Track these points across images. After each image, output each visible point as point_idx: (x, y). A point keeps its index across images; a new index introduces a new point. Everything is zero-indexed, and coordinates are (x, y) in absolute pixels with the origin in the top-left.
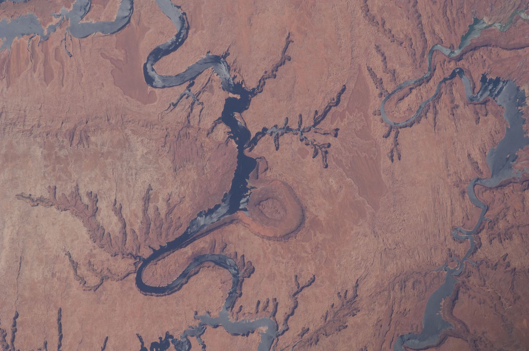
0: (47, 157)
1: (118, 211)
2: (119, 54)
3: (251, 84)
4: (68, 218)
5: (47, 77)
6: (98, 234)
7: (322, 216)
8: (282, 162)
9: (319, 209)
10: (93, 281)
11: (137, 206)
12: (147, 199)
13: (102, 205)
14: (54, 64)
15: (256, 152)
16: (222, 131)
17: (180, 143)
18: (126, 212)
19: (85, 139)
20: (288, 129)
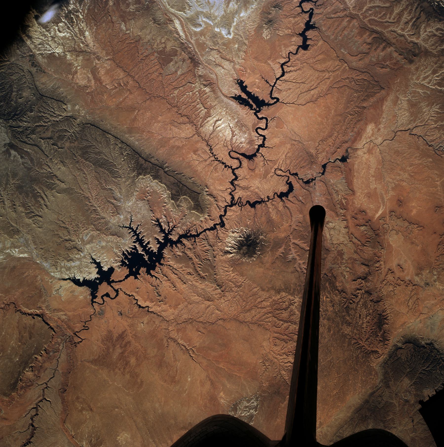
0: (236, 122)
1: (236, 140)
2: (256, 122)
3: (265, 146)
4: (231, 133)
5: (246, 114)
6: (232, 139)
7: (256, 172)
8: (258, 159)
9: (257, 171)
10: (225, 145)
11: (239, 142)
12: (241, 143)
13: (236, 136)
14: (249, 114)
15: (257, 154)
16: (257, 147)
17: (251, 142)
18: (237, 141)
19: (242, 126)
20: (263, 156)
